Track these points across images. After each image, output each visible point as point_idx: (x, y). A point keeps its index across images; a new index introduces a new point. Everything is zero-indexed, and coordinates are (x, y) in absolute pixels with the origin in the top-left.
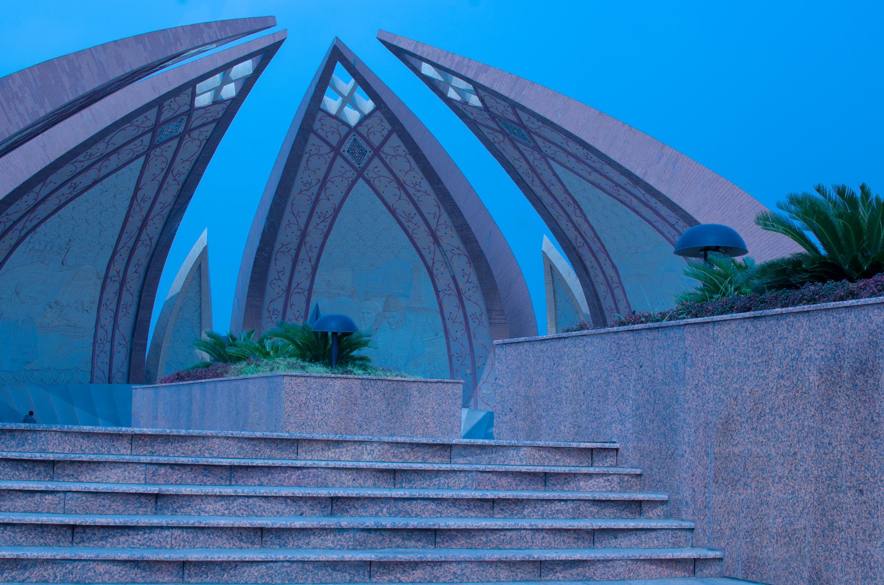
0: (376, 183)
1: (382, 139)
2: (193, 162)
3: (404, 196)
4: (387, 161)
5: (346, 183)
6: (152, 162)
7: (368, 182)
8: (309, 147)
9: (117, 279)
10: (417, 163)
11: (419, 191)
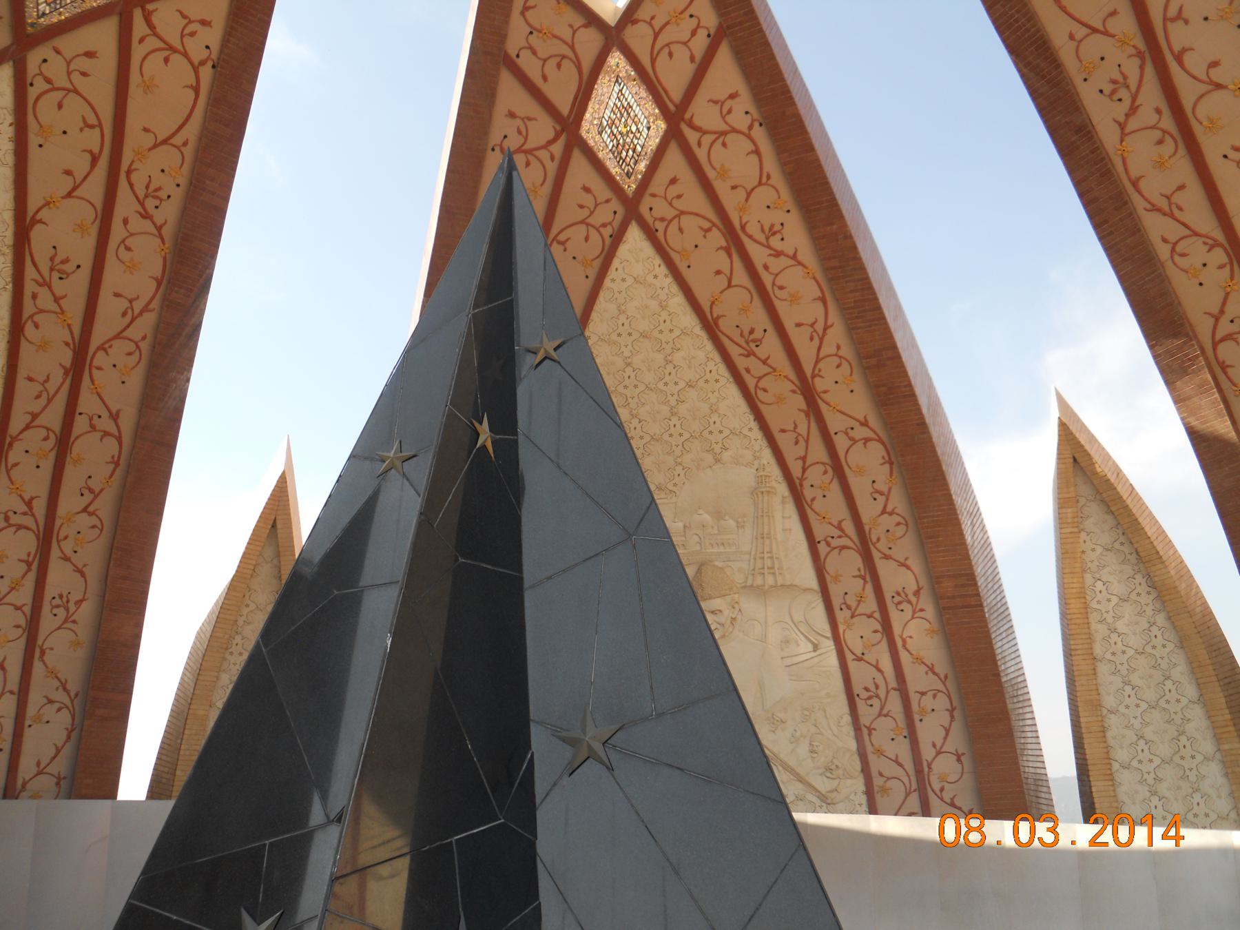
0: (674, 240)
1: (689, 69)
2: (189, 151)
3: (741, 276)
4: (701, 154)
5: (595, 246)
6: (45, 111)
7: (650, 234)
8: (502, 128)
9: (28, 521)
10: (781, 148)
11: (778, 254)
